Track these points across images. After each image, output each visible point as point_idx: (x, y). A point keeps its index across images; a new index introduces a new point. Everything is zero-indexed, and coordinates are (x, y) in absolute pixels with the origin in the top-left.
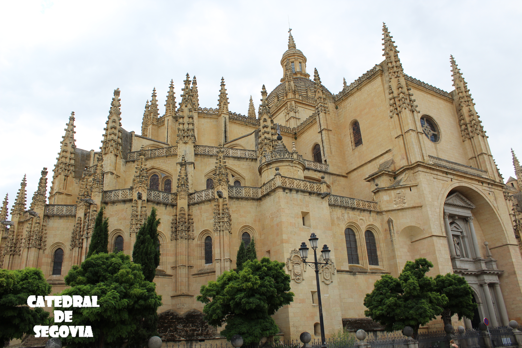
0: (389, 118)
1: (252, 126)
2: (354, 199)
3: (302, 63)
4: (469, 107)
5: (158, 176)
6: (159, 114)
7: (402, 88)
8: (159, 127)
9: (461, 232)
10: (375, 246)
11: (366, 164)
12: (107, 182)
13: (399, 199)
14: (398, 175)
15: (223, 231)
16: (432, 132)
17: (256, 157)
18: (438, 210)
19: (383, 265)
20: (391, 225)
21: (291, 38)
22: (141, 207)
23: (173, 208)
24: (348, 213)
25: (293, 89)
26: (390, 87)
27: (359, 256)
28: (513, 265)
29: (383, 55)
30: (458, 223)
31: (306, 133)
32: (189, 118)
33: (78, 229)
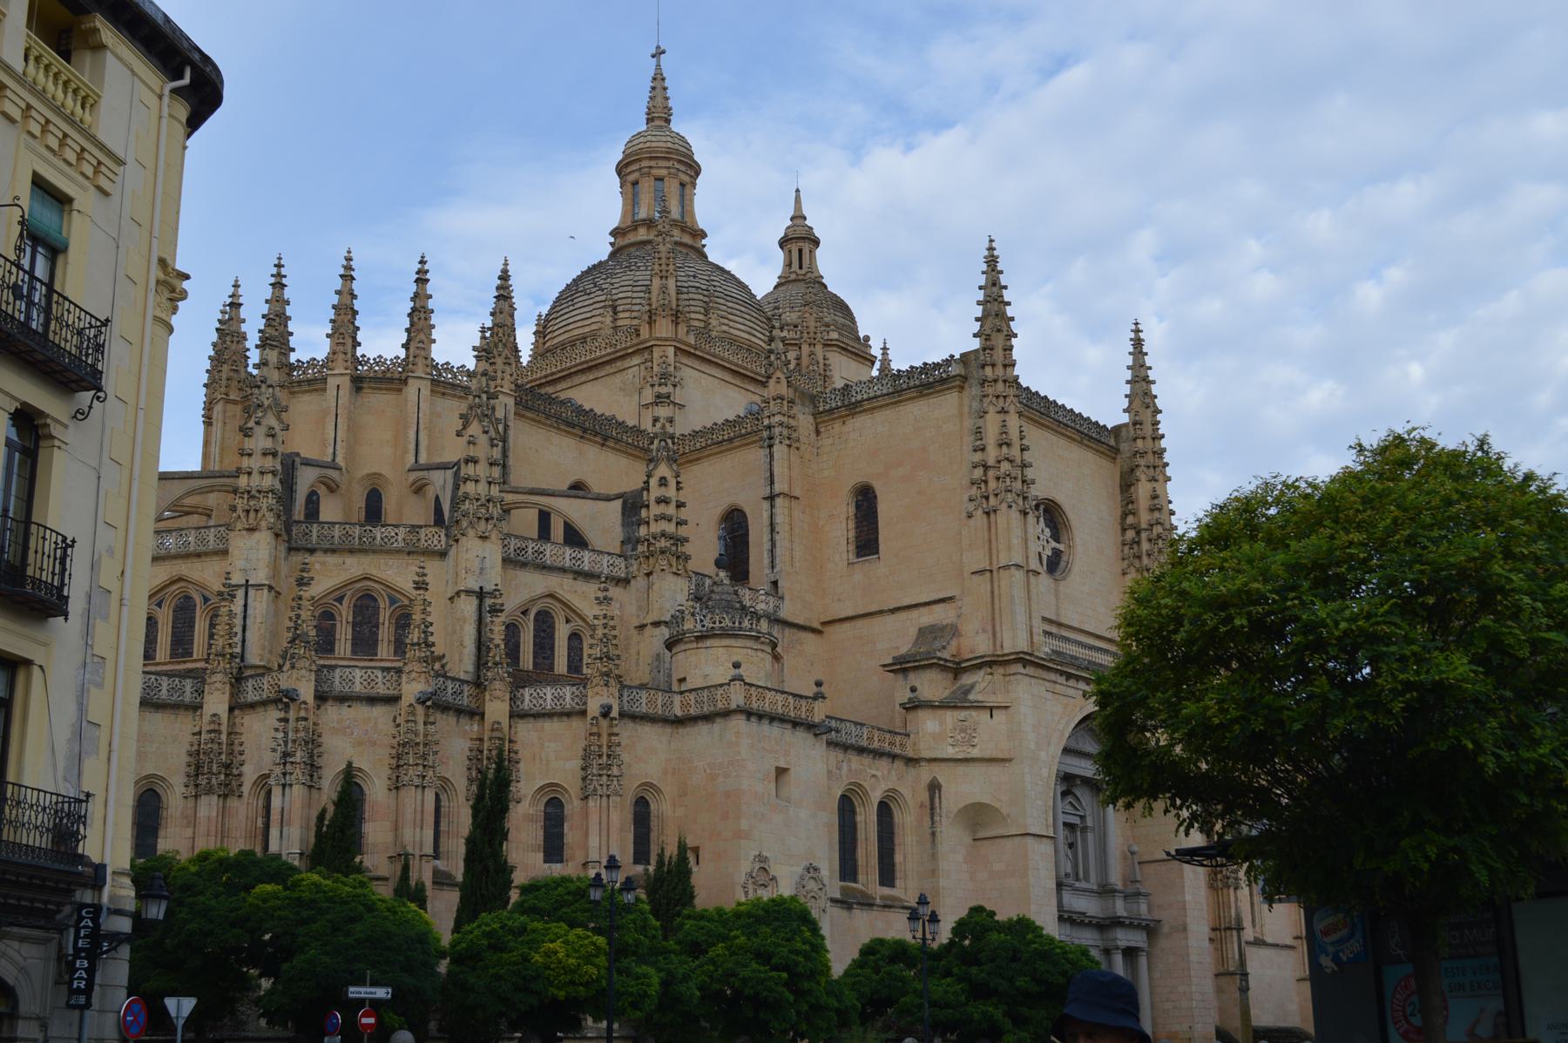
0: (965, 515)
1: (563, 427)
2: (862, 725)
3: (688, 186)
4: (1155, 484)
5: (376, 600)
6: (293, 350)
7: (1008, 445)
8: (293, 393)
9: (1081, 817)
10: (891, 840)
11: (881, 612)
12: (257, 611)
13: (963, 735)
14: (966, 670)
15: (608, 796)
16: (1054, 544)
17: (627, 573)
18: (1045, 772)
19: (906, 889)
20: (937, 795)
21: (658, 78)
22: (425, 724)
23: (471, 719)
24: (850, 761)
25: (674, 307)
26: (978, 432)
27: (860, 863)
28: (1184, 909)
29: (975, 335)
30: (1079, 795)
31: (706, 464)
32: (491, 464)
33: (215, 747)
